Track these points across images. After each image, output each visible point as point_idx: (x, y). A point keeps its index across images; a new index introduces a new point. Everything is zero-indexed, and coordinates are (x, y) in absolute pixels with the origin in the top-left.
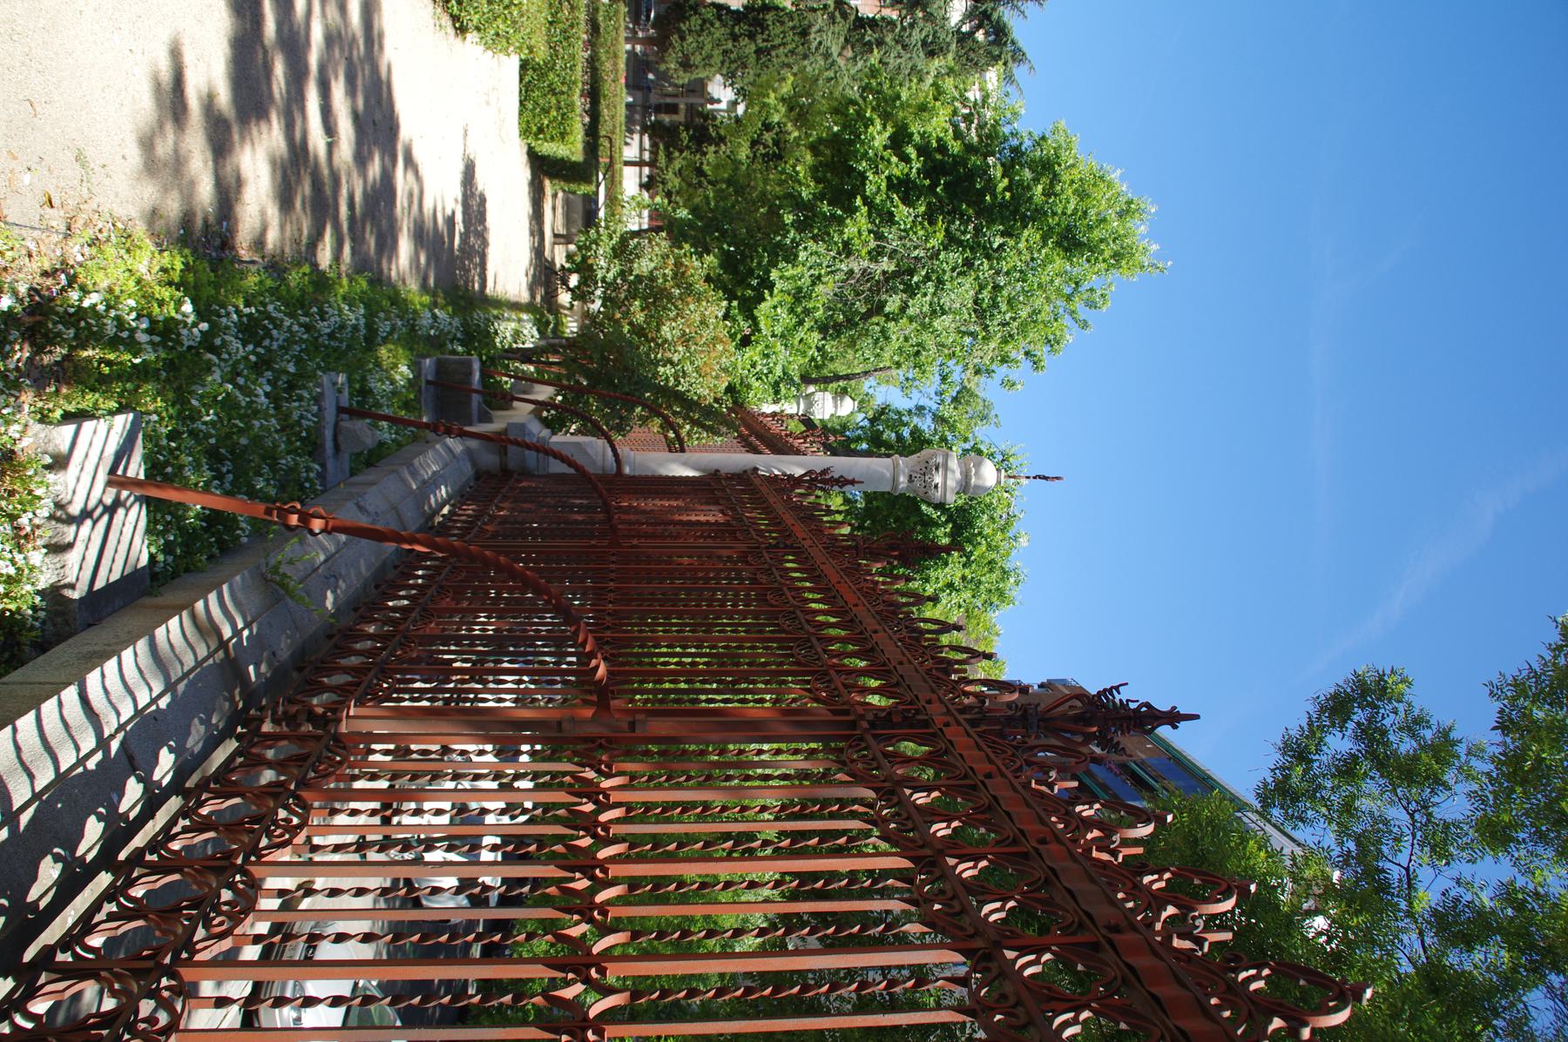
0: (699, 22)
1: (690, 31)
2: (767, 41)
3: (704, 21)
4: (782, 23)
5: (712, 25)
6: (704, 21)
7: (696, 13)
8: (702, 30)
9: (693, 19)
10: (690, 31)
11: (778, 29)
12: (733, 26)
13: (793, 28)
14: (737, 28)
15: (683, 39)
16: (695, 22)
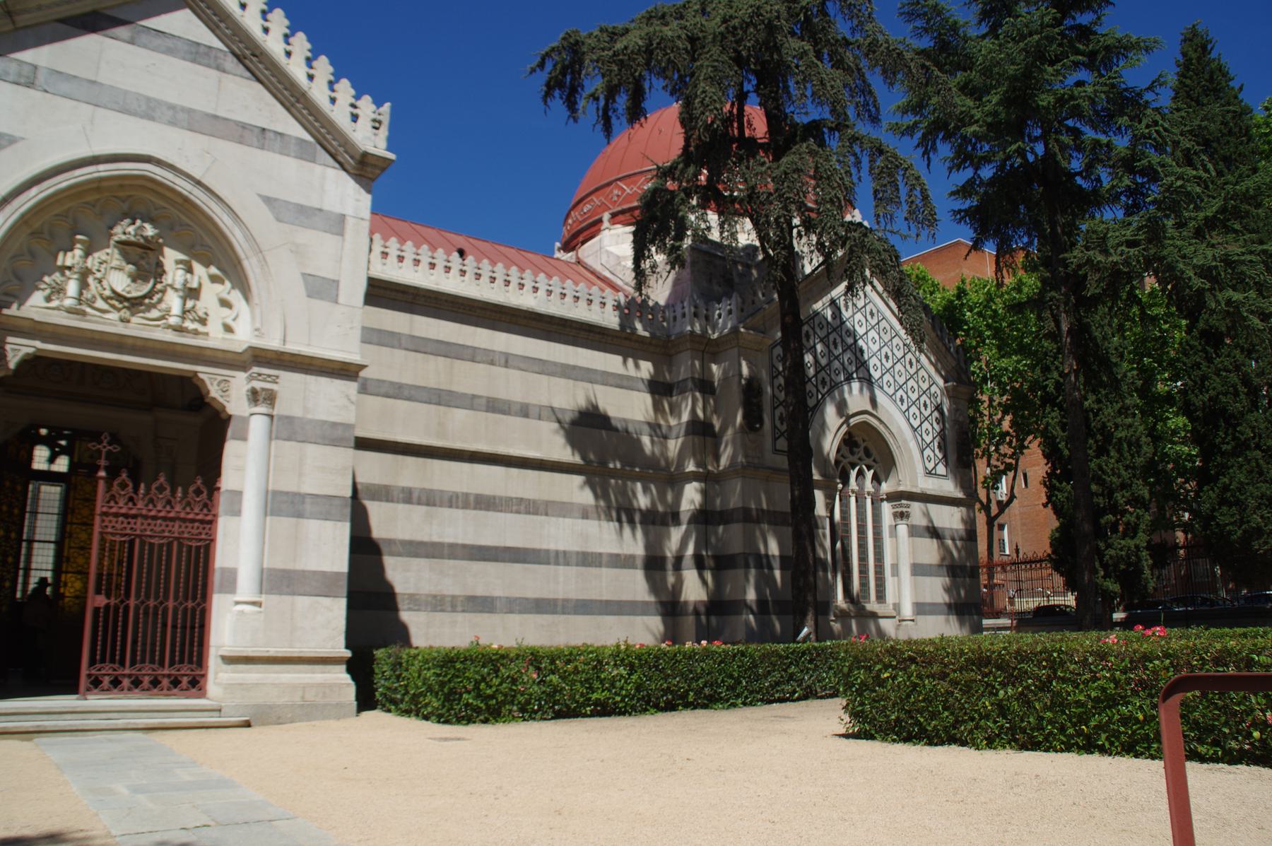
0: (1225, 509)
1: (1242, 522)
2: (1236, 394)
3: (1223, 502)
4: (1204, 378)
5: (1226, 488)
6: (1223, 502)
7: (1214, 518)
8: (1238, 503)
9: (1222, 520)
10: (1242, 522)
11: (1216, 382)
12: (1223, 454)
13: (1209, 360)
14: (1224, 447)
15: (1258, 532)
16: (1225, 517)
